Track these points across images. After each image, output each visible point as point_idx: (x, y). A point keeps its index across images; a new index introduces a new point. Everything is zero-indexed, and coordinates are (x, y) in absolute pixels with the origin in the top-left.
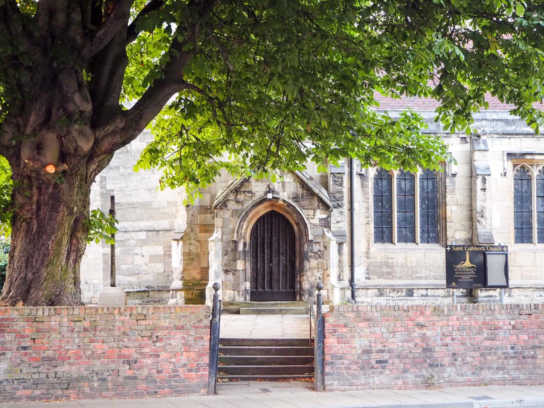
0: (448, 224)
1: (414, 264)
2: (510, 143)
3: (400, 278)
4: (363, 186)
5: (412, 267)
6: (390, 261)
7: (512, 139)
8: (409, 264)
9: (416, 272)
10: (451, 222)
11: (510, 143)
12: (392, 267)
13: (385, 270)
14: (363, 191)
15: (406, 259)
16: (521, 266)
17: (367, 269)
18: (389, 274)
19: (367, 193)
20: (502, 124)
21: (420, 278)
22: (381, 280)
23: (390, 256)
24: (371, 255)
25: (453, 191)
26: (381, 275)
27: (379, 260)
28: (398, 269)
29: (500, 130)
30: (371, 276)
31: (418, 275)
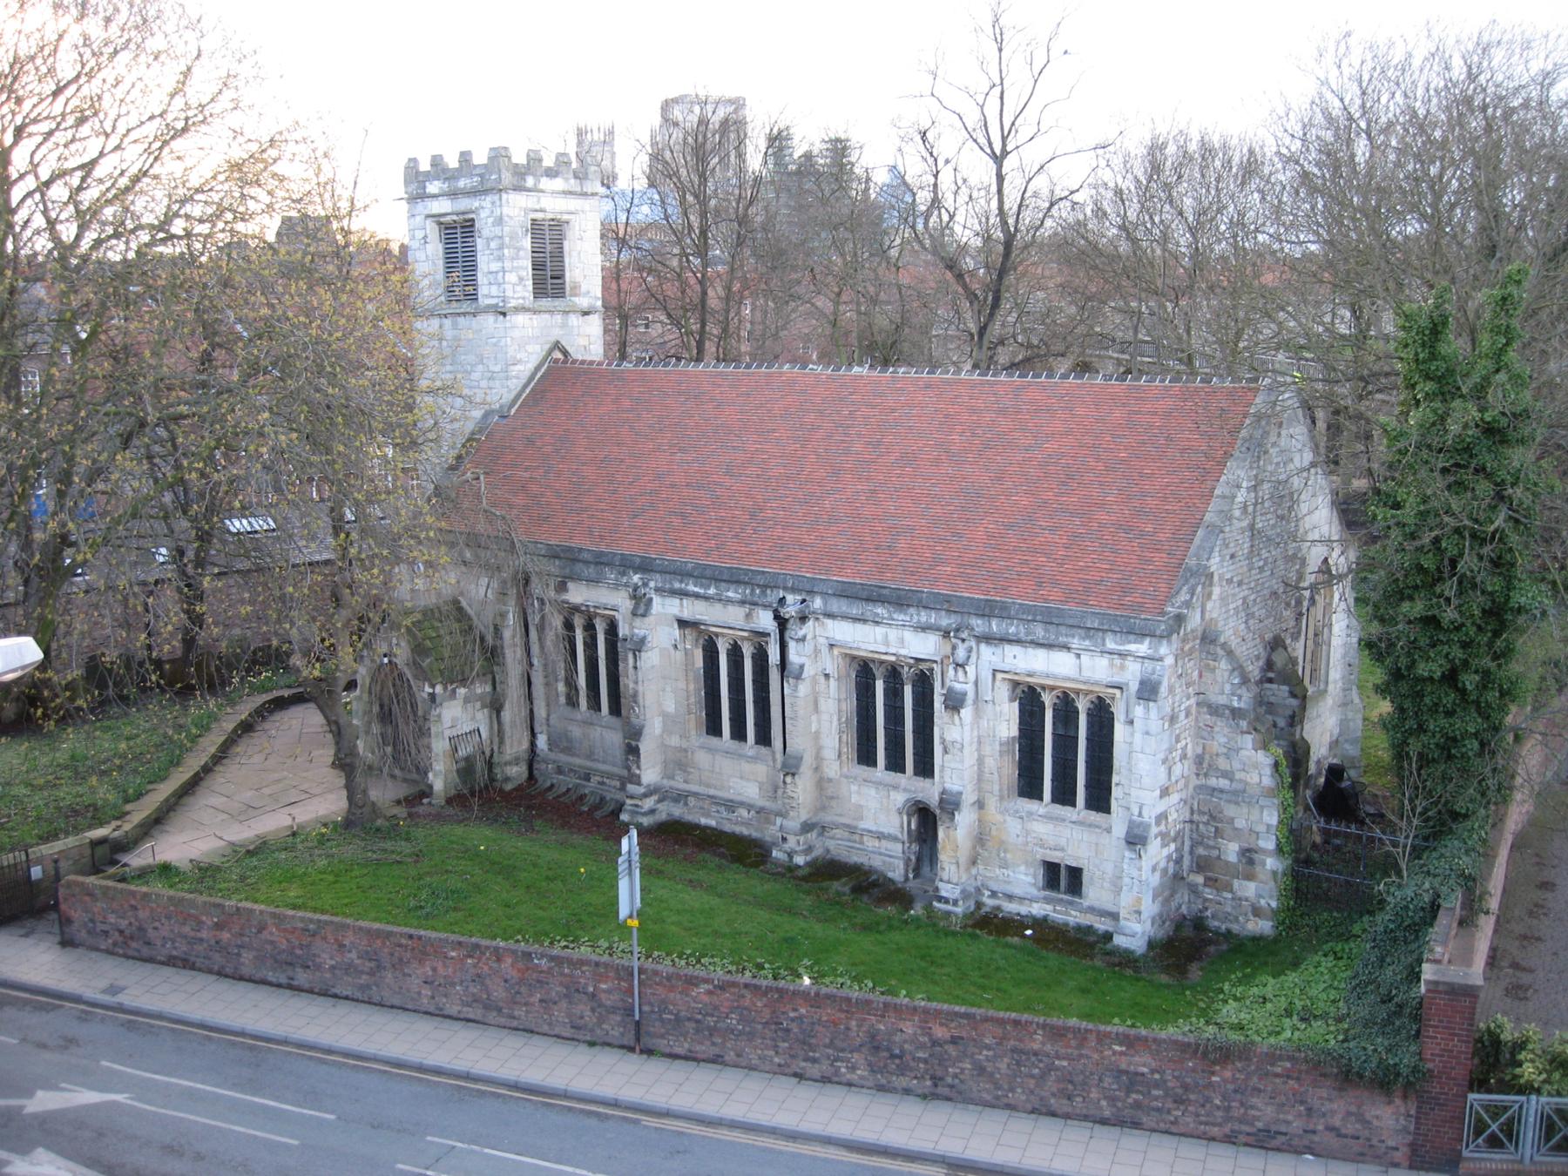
0: (622, 700)
2: (682, 605)
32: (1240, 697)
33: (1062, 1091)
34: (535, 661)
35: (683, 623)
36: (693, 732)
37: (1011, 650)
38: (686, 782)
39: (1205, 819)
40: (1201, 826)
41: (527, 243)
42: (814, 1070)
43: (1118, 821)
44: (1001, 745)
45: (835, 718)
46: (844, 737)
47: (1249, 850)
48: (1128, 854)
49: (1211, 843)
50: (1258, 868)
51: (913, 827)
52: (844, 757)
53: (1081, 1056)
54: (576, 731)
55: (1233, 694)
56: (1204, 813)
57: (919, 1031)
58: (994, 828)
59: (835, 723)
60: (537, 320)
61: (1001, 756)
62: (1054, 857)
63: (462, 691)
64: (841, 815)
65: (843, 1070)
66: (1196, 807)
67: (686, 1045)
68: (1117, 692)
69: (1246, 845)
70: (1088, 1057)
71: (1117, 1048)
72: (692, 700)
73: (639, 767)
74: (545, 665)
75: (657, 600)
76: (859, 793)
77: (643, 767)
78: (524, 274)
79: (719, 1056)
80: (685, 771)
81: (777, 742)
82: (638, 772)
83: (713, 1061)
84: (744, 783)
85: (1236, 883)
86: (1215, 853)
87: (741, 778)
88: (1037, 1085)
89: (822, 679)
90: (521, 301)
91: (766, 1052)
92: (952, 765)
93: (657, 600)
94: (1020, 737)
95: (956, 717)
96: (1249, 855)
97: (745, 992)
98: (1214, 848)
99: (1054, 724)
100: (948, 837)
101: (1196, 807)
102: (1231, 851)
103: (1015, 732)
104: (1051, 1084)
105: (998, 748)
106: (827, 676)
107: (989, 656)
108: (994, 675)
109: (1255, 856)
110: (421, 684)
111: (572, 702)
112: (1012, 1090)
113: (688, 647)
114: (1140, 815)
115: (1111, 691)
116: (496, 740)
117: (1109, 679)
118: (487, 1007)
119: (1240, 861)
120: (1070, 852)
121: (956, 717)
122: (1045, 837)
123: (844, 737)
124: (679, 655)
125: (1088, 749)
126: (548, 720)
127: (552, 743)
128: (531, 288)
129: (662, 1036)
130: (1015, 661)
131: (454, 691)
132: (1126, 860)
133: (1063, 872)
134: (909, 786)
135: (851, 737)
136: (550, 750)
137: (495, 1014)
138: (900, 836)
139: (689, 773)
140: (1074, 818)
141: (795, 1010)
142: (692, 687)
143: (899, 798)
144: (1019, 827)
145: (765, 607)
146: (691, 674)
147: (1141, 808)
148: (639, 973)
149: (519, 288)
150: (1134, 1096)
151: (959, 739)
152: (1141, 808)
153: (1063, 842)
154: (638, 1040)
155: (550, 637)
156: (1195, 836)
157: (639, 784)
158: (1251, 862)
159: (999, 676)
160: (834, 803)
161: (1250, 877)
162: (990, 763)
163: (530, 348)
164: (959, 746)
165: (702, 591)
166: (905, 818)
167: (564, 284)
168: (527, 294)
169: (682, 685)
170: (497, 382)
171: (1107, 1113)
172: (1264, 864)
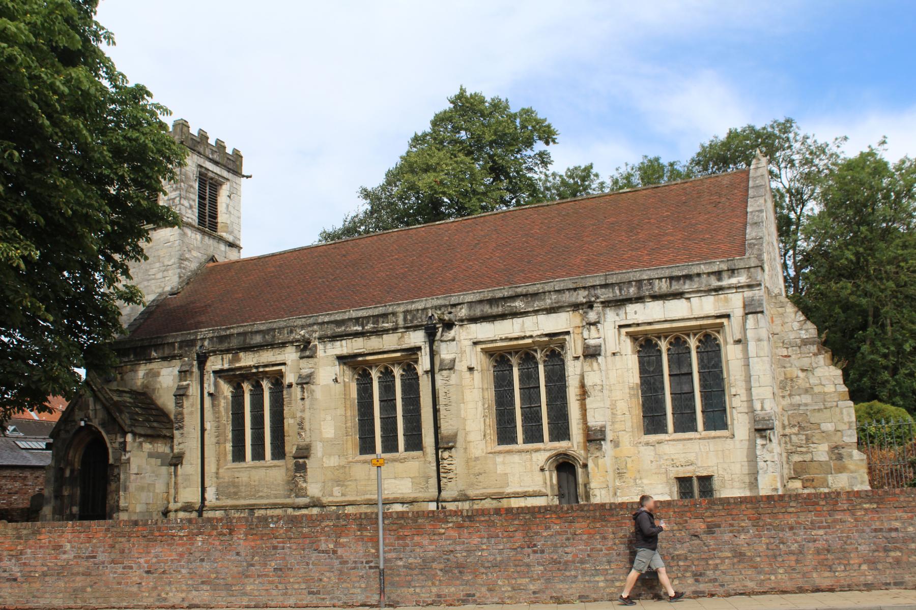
0: (286, 438)
1: (256, 483)
2: (342, 346)
3: (245, 498)
4: (213, 405)
5: (255, 486)
6: (236, 480)
7: (344, 342)
8: (252, 483)
9: (259, 491)
10: (289, 436)
11: (342, 346)
12: (237, 487)
13: (232, 490)
14: (213, 410)
15: (249, 477)
16: (356, 480)
17: (217, 490)
18: (235, 493)
19: (219, 412)
20: (333, 326)
21: (261, 497)
22: (228, 501)
23: (236, 476)
24: (221, 475)
25: (290, 403)
26: (229, 496)
27: (226, 480)
28: (243, 489)
29: (329, 333)
30: (220, 497)
31: (260, 494)
32: (807, 330)
33: (821, 563)
34: (208, 426)
35: (341, 359)
36: (350, 452)
37: (631, 308)
38: (343, 495)
39: (795, 430)
40: (793, 437)
41: (196, 185)
42: (575, 589)
43: (740, 424)
44: (630, 388)
45: (480, 404)
46: (488, 420)
47: (836, 447)
48: (760, 442)
49: (802, 449)
50: (846, 461)
51: (555, 481)
52: (488, 438)
53: (835, 521)
54: (244, 477)
55: (801, 329)
56: (794, 426)
57: (676, 528)
58: (629, 460)
59: (480, 408)
60: (199, 236)
61: (630, 397)
62: (684, 472)
63: (147, 446)
64: (490, 487)
65: (601, 584)
66: (786, 423)
67: (434, 590)
68: (725, 321)
69: (834, 444)
70: (842, 521)
71: (866, 506)
72: (349, 424)
73: (305, 481)
74: (218, 427)
75: (320, 347)
76: (504, 463)
77: (309, 480)
78: (193, 203)
79: (469, 595)
80: (342, 486)
81: (428, 439)
82: (304, 485)
83: (464, 602)
84: (397, 482)
85: (830, 478)
86: (808, 457)
87: (395, 478)
88: (797, 561)
89: (467, 374)
90: (190, 220)
91: (519, 581)
92: (595, 406)
93: (320, 347)
94: (642, 384)
95: (595, 364)
96: (837, 452)
97: (495, 518)
98: (807, 453)
99: (669, 367)
100: (597, 465)
101: (786, 423)
102: (821, 452)
103: (637, 380)
104: (810, 559)
105: (627, 391)
106: (471, 369)
107: (612, 318)
108: (619, 331)
109: (842, 451)
110: (114, 436)
111: (239, 455)
112: (774, 573)
113: (347, 380)
114: (763, 409)
115: (718, 321)
116: (172, 491)
117: (716, 312)
118: (215, 587)
119: (831, 458)
120: (699, 465)
121: (595, 364)
122: (676, 456)
123: (488, 420)
124: (339, 387)
125: (700, 380)
126: (217, 473)
127: (218, 493)
128: (197, 215)
129: (409, 584)
130: (636, 316)
131: (141, 443)
132: (759, 447)
133: (695, 483)
134: (548, 448)
135: (492, 421)
136: (217, 499)
137: (224, 593)
138: (544, 490)
139: (347, 486)
140: (698, 436)
141: (548, 528)
142: (349, 413)
143: (541, 458)
144: (652, 453)
145: (416, 328)
146: (348, 402)
147: (762, 403)
148: (384, 518)
149: (190, 211)
150: (892, 554)
151: (599, 382)
152: (762, 403)
153: (692, 457)
154: (382, 591)
155: (223, 403)
156: (789, 447)
157: (305, 496)
158: (840, 457)
159: (624, 331)
160: (481, 478)
161: (841, 469)
162: (622, 406)
163: (195, 253)
164: (600, 388)
165: (359, 328)
166: (547, 473)
167: (217, 223)
168: (194, 217)
169: (341, 411)
170: (170, 272)
171: (870, 579)
172: (851, 456)
